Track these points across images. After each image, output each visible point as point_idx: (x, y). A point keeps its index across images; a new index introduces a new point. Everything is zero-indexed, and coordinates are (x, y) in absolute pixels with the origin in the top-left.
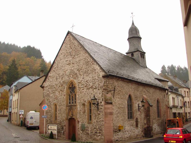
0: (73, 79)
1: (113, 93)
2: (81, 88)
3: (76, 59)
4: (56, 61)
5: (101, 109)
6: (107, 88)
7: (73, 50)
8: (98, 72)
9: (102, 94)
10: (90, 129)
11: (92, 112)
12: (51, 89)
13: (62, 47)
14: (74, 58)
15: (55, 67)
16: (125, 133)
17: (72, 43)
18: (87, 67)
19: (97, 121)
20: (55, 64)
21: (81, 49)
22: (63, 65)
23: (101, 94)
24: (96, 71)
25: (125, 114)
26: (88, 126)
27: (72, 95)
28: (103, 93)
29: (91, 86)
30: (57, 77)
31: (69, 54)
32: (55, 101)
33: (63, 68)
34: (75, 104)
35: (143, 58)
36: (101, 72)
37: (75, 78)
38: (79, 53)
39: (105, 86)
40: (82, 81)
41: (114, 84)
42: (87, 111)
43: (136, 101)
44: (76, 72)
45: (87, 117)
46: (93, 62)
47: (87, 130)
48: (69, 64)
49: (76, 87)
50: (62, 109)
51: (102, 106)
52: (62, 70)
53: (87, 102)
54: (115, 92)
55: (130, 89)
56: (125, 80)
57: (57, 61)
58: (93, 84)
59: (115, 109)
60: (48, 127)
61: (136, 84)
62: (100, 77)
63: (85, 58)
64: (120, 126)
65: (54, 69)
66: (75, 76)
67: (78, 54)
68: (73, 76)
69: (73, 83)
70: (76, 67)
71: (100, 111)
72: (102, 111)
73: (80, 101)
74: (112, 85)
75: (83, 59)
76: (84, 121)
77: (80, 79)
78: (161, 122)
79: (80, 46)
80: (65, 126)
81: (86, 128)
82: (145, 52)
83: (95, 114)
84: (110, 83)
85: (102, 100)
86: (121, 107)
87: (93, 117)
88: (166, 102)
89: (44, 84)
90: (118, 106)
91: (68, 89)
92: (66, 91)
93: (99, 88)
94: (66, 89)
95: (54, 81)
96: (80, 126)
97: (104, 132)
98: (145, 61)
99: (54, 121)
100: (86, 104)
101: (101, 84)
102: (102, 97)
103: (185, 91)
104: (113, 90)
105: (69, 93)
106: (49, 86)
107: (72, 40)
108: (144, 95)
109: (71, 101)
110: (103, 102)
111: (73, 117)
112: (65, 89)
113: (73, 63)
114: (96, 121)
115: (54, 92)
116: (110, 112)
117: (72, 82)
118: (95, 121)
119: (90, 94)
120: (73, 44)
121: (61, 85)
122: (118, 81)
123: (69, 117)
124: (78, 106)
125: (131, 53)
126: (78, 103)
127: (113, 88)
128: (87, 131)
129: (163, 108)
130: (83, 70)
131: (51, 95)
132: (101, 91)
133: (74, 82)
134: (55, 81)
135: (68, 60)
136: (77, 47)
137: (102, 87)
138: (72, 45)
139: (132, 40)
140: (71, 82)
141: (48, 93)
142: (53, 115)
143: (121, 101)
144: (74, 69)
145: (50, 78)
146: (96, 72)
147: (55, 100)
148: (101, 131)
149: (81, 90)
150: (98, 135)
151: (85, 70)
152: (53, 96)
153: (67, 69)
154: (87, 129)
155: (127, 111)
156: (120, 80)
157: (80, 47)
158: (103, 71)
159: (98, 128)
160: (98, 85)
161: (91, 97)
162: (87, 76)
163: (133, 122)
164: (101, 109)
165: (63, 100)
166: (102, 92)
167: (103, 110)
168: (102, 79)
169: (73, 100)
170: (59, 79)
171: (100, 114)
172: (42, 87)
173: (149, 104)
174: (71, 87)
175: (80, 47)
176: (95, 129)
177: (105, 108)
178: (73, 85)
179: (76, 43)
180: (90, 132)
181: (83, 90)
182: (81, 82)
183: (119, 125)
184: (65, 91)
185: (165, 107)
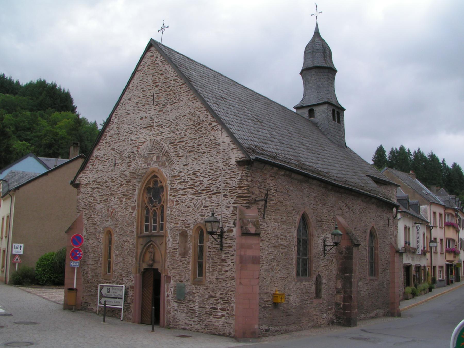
0: (159, 168)
1: (263, 208)
2: (177, 191)
3: (168, 113)
4: (113, 118)
5: (231, 247)
6: (248, 193)
7: (160, 90)
8: (226, 150)
9: (234, 207)
10: (197, 299)
11: (206, 254)
12: (100, 190)
13: (133, 81)
15: (112, 132)
17: (161, 73)
18: (198, 137)
19: (217, 279)
20: (111, 126)
21: (183, 89)
22: (134, 129)
23: (232, 208)
24: (221, 148)
25: (290, 262)
26: (194, 291)
27: (153, 208)
28: (235, 205)
29: (205, 186)
30: (116, 160)
31: (149, 100)
32: (108, 223)
33: (133, 138)
34: (161, 233)
35: (339, 122)
36: (234, 151)
37: (163, 165)
38: (178, 98)
39: (242, 187)
40: (181, 172)
41: (267, 184)
42: (191, 252)
43: (320, 230)
44: (167, 148)
45: (191, 266)
46: (214, 124)
47: (190, 301)
48: (150, 127)
49: (165, 188)
50: (126, 243)
51: (232, 239)
52: (130, 142)
53: (194, 227)
54: (268, 204)
55: (306, 199)
56: (293, 175)
57: (117, 118)
58: (210, 182)
59: (267, 248)
61: (320, 186)
62: (229, 165)
63: (192, 111)
65: (108, 138)
66: (165, 158)
67: (175, 101)
68: (158, 157)
69: (156, 176)
70: (167, 133)
71: (225, 253)
72: (232, 253)
73: (175, 225)
74: (262, 187)
75: (187, 115)
76: (184, 277)
77: (178, 168)
78: (377, 287)
79: (181, 81)
80: (132, 288)
81: (189, 294)
82: (344, 106)
83: (213, 259)
84: (255, 180)
85: (234, 224)
86: (281, 245)
87: (207, 266)
88: (391, 238)
89: (80, 176)
90: (274, 241)
91: (143, 194)
92: (139, 199)
93: (228, 194)
94: (139, 193)
95: (106, 169)
96: (172, 289)
97: (234, 308)
98: (342, 130)
99: (104, 275)
100: (190, 233)
101: (231, 182)
102: (235, 217)
103: (434, 213)
104: (262, 200)
105: (146, 203)
106: (94, 181)
107: (160, 64)
109: (151, 224)
110: (234, 230)
111: (155, 266)
114: (214, 277)
115: (107, 199)
118: (211, 277)
119: (202, 208)
120: (162, 74)
121: (125, 181)
122: (277, 177)
123: (145, 266)
124: (170, 238)
125: (309, 109)
126: (169, 231)
127: (263, 195)
128: (191, 303)
129: (384, 254)
130: (186, 143)
131: (98, 207)
132: (233, 201)
133: (161, 174)
134: (110, 169)
135: (147, 115)
136: (172, 82)
137: (236, 189)
138: (159, 76)
140: (152, 175)
141: (90, 202)
142: (102, 260)
143: (283, 229)
144: (161, 140)
145: (96, 161)
146: (221, 151)
147: (109, 219)
148: (227, 305)
149: (179, 196)
150: (220, 314)
151: (191, 144)
152: (104, 208)
153: (144, 140)
154: (191, 297)
155: (295, 257)
156: (282, 175)
157: (181, 82)
159: (221, 296)
160: (224, 185)
161: (204, 215)
162: (196, 159)
164: (228, 249)
165: (130, 222)
166: (233, 204)
167: (235, 251)
168: (237, 170)
169: (155, 221)
170: (121, 164)
171: (227, 260)
172: (76, 185)
173: (351, 240)
174: (151, 186)
175: (181, 82)
176: (212, 299)
177: (242, 246)
178: (156, 182)
179: (170, 72)
180: (197, 307)
181: (183, 195)
182: (180, 174)
183: (272, 292)
184: (136, 197)
185: (388, 249)
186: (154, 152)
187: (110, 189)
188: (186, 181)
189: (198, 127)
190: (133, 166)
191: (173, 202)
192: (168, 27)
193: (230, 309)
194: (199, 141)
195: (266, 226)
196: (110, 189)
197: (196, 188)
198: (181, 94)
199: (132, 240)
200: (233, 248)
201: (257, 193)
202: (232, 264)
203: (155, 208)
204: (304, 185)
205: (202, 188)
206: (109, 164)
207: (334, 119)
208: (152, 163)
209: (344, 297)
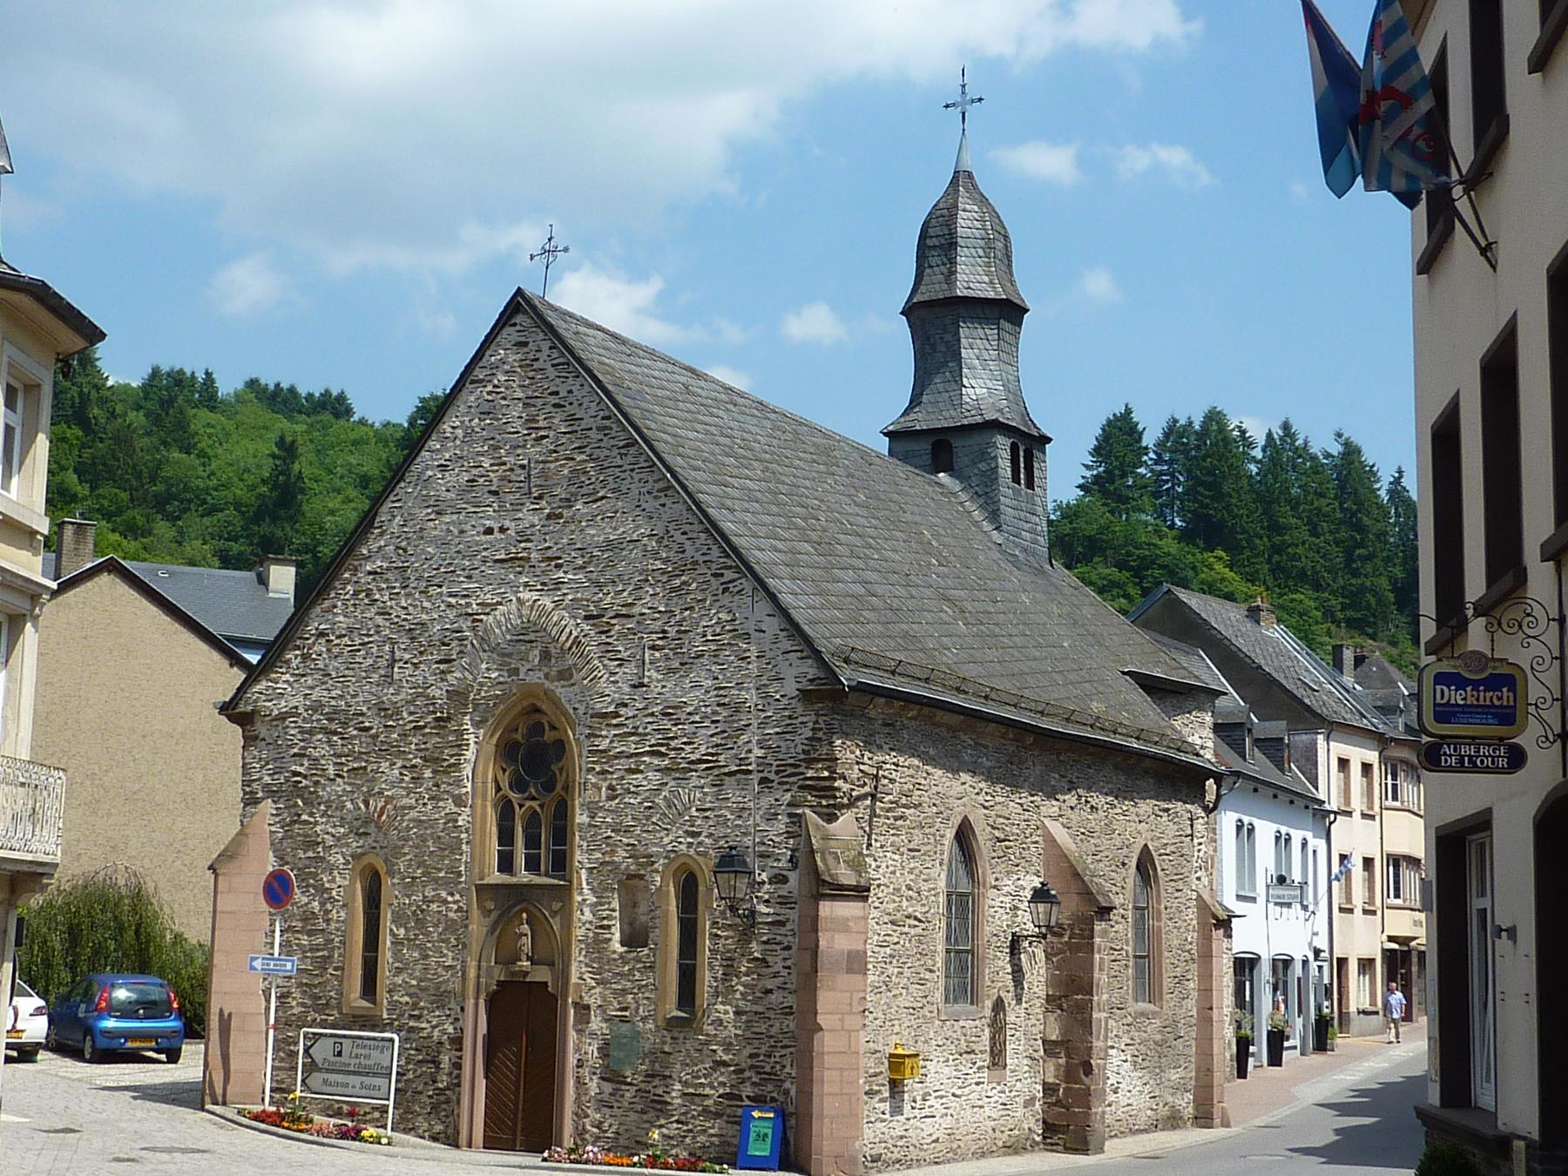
0: (547, 684)
8: (769, 654)
14: (560, 516)
16: (924, 1113)
21: (630, 459)
27: (528, 804)
29: (703, 750)
40: (626, 705)
46: (729, 575)
50: (434, 907)
56: (940, 715)
60: (306, 1051)
63: (659, 531)
64: (904, 1056)
68: (546, 656)
69: (538, 710)
85: (790, 861)
86: (908, 917)
88: (1199, 879)
93: (772, 776)
101: (782, 744)
108: (1046, 821)
110: (793, 877)
112: (470, 754)
113: (549, 553)
116: (850, 952)
117: (531, 701)
128: (656, 1082)
133: (556, 703)
135: (507, 524)
139: (947, 321)
140: (525, 704)
147: (372, 829)
148: (770, 1087)
155: (941, 948)
158: (817, 655)
161: (699, 834)
162: (674, 671)
163: (976, 1026)
164: (774, 929)
168: (800, 710)
173: (1087, 894)
174: (519, 737)
178: (537, 729)
186: (532, 637)
187: (375, 737)
188: (640, 730)
189: (677, 582)
190: (458, 675)
191: (600, 789)
192: (566, 250)
193: (781, 1099)
194: (684, 619)
195: (874, 865)
196: (375, 737)
197: (672, 754)
198: (623, 475)
199: (457, 897)
200: (789, 926)
201: (854, 774)
202: (784, 972)
203: (535, 804)
204: (963, 737)
205: (693, 757)
206: (371, 661)
207: (1016, 479)
208: (523, 670)
209: (1068, 1067)
